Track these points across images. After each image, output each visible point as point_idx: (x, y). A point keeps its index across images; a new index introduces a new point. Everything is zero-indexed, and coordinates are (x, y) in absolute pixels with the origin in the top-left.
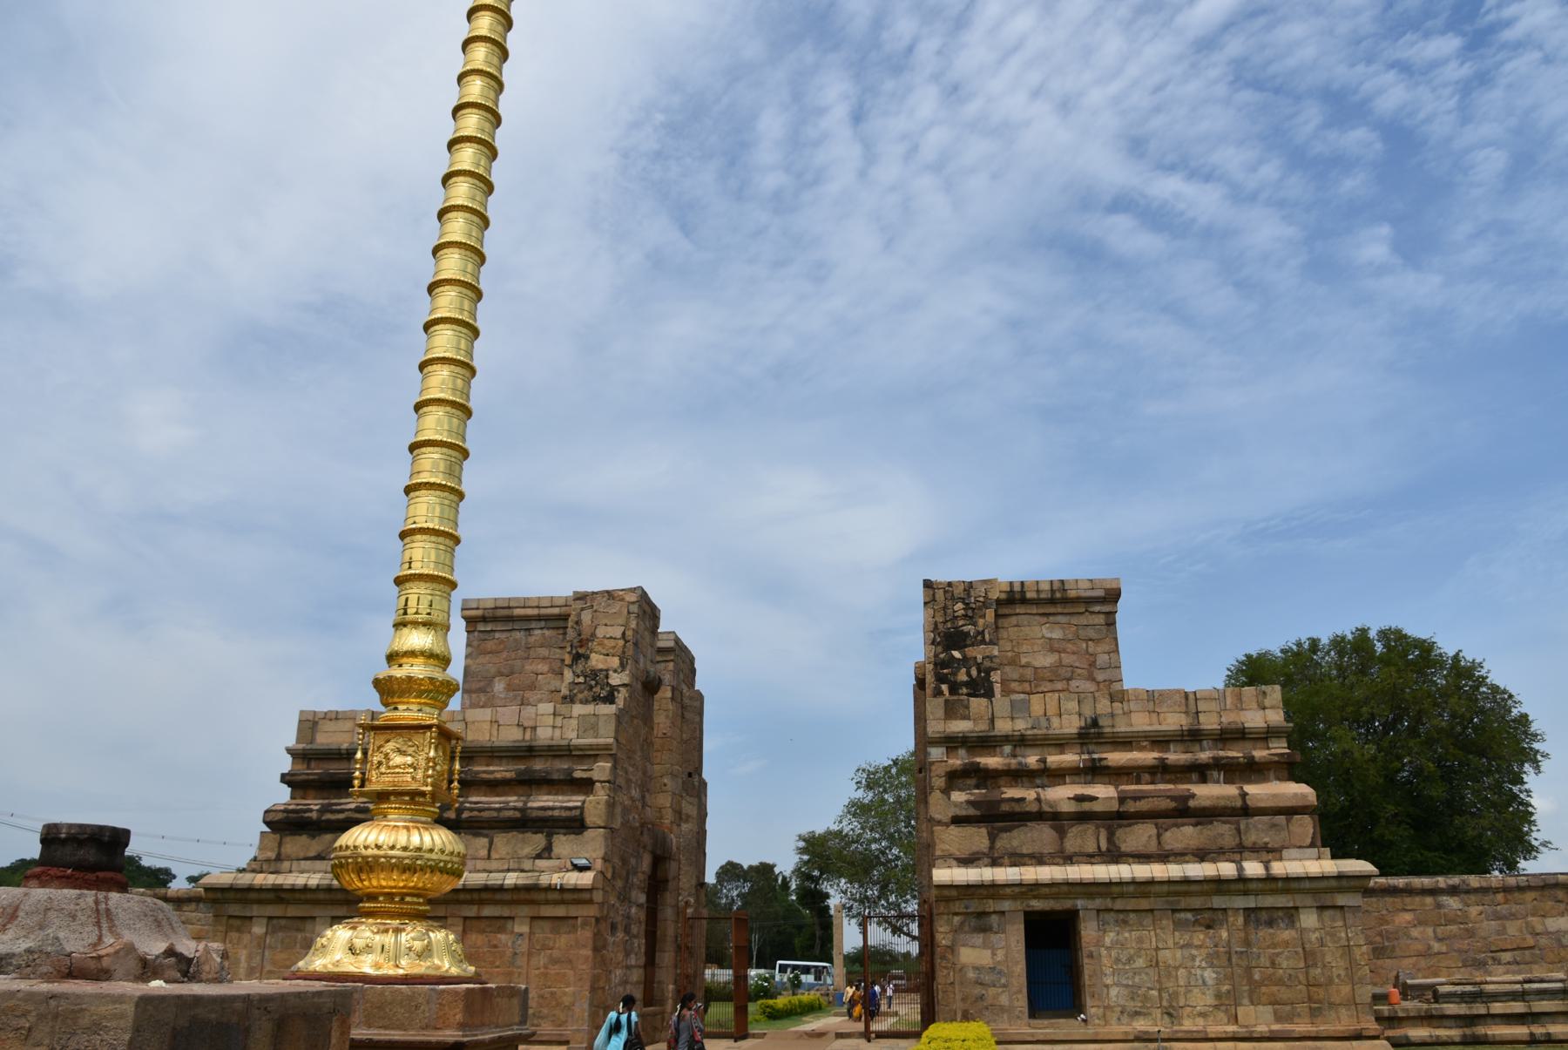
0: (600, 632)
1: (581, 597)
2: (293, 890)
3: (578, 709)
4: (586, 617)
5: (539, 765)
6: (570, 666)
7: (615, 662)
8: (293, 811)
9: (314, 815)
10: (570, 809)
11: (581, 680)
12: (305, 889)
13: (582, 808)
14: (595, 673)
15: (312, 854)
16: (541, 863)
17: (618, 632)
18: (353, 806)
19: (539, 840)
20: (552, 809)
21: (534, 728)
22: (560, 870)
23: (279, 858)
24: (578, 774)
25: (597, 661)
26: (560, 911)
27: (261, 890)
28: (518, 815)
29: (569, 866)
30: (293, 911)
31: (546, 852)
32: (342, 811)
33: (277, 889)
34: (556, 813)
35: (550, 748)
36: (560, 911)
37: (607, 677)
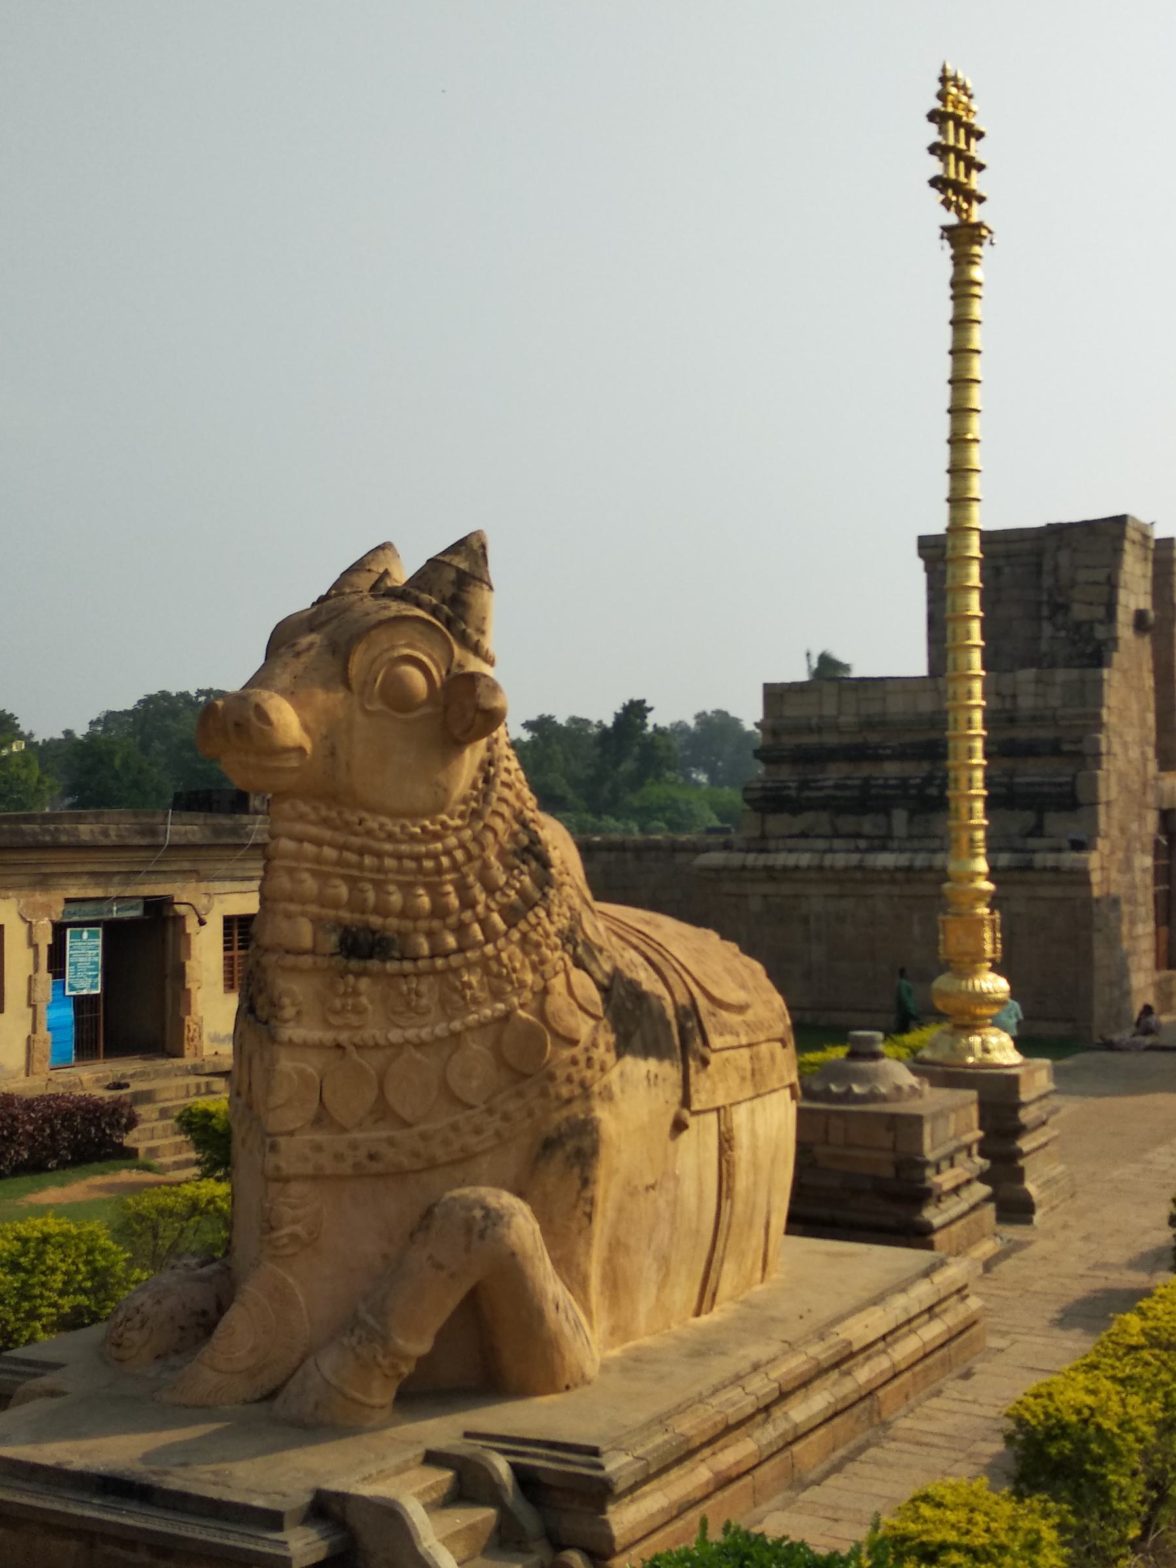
0: (1082, 576)
1: (1057, 531)
2: (785, 869)
3: (1061, 675)
4: (1064, 558)
5: (1022, 734)
6: (1050, 618)
7: (1100, 612)
8: (770, 789)
9: (793, 793)
10: (1060, 785)
11: (1063, 634)
12: (797, 868)
13: (1073, 784)
14: (1079, 625)
15: (796, 830)
16: (1033, 843)
17: (1101, 575)
18: (830, 783)
19: (1029, 817)
20: (1040, 784)
21: (1014, 696)
22: (1059, 850)
23: (764, 837)
24: (1066, 747)
25: (1079, 612)
26: (1057, 892)
27: (754, 869)
28: (1004, 790)
29: (1065, 844)
30: (786, 889)
31: (1037, 831)
32: (821, 788)
33: (769, 869)
34: (1046, 789)
35: (1034, 718)
36: (1057, 892)
37: (1092, 629)
